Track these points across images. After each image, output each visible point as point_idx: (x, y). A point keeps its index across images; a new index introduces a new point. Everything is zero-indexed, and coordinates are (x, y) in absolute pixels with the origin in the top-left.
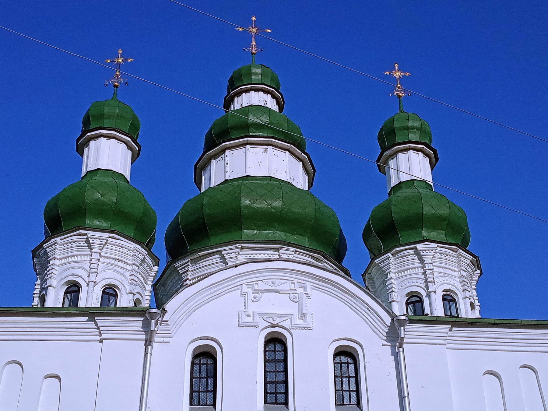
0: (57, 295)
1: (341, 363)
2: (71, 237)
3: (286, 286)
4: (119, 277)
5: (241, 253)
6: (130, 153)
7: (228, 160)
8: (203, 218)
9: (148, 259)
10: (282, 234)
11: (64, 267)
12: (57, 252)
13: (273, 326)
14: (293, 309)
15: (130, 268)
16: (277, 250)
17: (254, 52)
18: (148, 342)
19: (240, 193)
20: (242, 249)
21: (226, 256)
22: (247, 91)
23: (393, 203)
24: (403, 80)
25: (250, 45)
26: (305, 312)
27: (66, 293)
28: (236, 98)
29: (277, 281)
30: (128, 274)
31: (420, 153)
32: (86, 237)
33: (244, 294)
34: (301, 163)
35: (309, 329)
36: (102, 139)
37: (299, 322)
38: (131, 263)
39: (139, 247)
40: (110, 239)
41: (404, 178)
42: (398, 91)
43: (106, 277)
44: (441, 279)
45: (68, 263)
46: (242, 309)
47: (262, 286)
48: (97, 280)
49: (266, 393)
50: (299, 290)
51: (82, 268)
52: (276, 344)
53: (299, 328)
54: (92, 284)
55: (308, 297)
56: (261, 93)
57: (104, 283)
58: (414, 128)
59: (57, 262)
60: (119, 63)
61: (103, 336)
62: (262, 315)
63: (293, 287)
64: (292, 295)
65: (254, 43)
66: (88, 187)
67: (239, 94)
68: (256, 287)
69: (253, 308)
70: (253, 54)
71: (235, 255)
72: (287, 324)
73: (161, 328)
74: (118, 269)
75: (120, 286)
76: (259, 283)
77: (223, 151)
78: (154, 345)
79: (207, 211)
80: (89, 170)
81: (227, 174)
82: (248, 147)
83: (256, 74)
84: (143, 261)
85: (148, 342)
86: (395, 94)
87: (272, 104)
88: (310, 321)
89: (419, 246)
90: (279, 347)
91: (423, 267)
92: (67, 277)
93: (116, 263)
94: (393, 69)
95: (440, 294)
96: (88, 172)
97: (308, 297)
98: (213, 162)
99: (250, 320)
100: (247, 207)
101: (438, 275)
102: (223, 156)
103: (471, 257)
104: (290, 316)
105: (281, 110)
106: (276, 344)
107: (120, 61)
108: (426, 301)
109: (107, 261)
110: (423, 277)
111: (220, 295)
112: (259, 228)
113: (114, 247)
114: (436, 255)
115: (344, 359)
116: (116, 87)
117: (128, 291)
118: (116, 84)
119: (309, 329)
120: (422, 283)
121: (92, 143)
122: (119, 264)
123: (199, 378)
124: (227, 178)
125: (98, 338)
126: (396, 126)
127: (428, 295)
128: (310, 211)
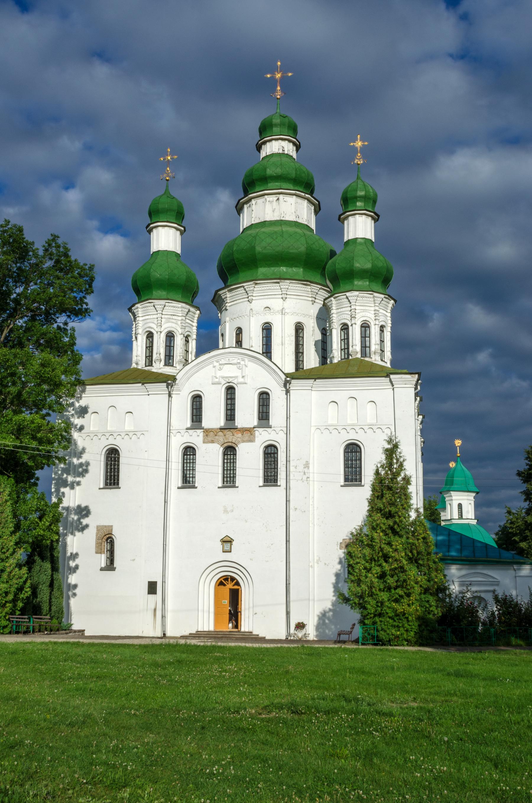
0: (143, 339)
1: (263, 399)
2: (146, 304)
3: (235, 361)
4: (174, 325)
5: (256, 286)
6: (178, 233)
7: (254, 207)
8: (234, 260)
9: (192, 309)
10: (284, 269)
11: (144, 318)
12: (140, 312)
13: (229, 383)
14: (238, 373)
15: (180, 318)
16: (278, 283)
17: (278, 97)
18: (170, 395)
19: (255, 244)
20: (256, 284)
21: (247, 290)
22: (270, 141)
23: (337, 261)
24: (363, 148)
25: (275, 90)
26: (244, 375)
27: (147, 337)
28: (263, 146)
29: (231, 359)
30: (179, 322)
31: (364, 216)
32: (152, 304)
33: (214, 367)
34: (306, 201)
35: (246, 383)
36: (160, 228)
37: (241, 380)
38: (181, 315)
39: (184, 305)
40: (167, 304)
41: (351, 237)
42: (357, 159)
43: (167, 326)
44: (361, 314)
45: (146, 319)
46: (214, 374)
47: (223, 362)
48: (162, 330)
49: (227, 415)
50: (242, 363)
51: (153, 323)
52: (230, 391)
53: (241, 383)
54: (159, 333)
55: (246, 366)
56: (280, 141)
57: (166, 330)
58: (361, 197)
59: (141, 319)
60: (168, 160)
61: (150, 393)
62: (223, 377)
63: (239, 361)
64: (238, 366)
65: (279, 88)
66: (152, 270)
67: (265, 143)
68: (221, 362)
69: (219, 374)
70: (278, 99)
71: (252, 289)
72: (235, 381)
73: (175, 387)
74: (173, 321)
75: (175, 331)
76: (222, 360)
77: (250, 200)
78: (173, 396)
79: (236, 256)
80: (154, 251)
81: (253, 219)
82: (266, 196)
83: (276, 125)
84: (189, 311)
85: (170, 395)
86: (356, 162)
87: (289, 148)
88: (246, 379)
89: (348, 294)
90: (233, 390)
91: (351, 307)
92: (146, 328)
93: (172, 317)
94: (355, 140)
95: (359, 323)
96: (154, 253)
97: (246, 366)
98: (245, 206)
99: (217, 380)
100: (259, 253)
101: (359, 311)
102: (250, 203)
103: (383, 296)
104: (236, 377)
105: (298, 147)
106: (230, 391)
107: (169, 158)
108: (350, 328)
109: (166, 316)
110: (350, 313)
111: (203, 368)
112: (269, 266)
113: (170, 308)
114: (358, 299)
115: (265, 396)
116: (167, 180)
117: (180, 333)
118: (167, 178)
119: (246, 383)
120: (349, 317)
121: (154, 230)
122: (174, 317)
123: (196, 409)
124: (253, 223)
125: (147, 393)
126: (348, 196)
127: (352, 325)
128: (303, 249)
